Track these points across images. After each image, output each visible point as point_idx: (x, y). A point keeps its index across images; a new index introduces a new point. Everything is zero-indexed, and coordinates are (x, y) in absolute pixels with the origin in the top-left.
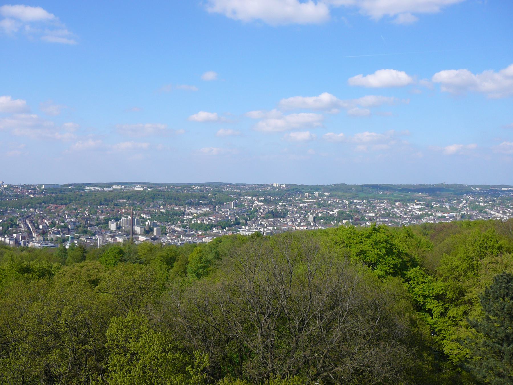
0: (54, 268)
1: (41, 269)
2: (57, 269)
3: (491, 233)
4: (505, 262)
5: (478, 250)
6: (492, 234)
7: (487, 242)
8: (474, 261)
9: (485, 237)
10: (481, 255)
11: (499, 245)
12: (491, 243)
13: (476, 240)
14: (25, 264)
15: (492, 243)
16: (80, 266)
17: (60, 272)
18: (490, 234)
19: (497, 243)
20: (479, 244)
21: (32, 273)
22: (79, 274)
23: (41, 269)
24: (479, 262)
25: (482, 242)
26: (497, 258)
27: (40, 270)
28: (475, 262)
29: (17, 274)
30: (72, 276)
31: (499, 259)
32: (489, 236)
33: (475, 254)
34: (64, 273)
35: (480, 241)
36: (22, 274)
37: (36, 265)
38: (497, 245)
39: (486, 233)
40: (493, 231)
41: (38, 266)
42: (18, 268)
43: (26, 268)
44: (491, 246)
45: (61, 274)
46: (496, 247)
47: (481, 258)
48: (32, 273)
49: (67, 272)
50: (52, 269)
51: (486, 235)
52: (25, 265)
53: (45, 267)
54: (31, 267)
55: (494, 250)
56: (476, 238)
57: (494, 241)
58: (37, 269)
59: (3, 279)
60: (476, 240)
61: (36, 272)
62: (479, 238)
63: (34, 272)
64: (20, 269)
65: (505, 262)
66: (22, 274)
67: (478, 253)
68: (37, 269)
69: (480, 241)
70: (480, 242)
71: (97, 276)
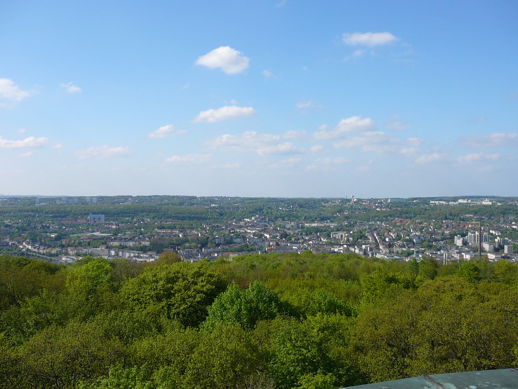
0: (418, 280)
1: (405, 280)
2: (420, 282)
14: (391, 275)
16: (443, 281)
17: (423, 285)
21: (398, 283)
22: (443, 288)
23: (405, 280)
27: (404, 281)
29: (384, 283)
30: (436, 290)
34: (428, 286)
36: (388, 283)
37: (401, 277)
41: (403, 277)
42: (385, 277)
43: (391, 278)
45: (424, 286)
48: (398, 283)
49: (430, 285)
50: (416, 281)
52: (391, 276)
53: (409, 279)
54: (396, 278)
58: (402, 280)
59: (371, 286)
61: (401, 283)
63: (399, 283)
64: (387, 279)
66: (389, 283)
68: (402, 280)
71: (462, 292)
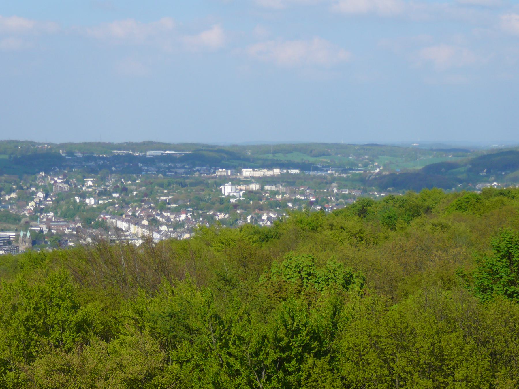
3: (58, 285)
4: (90, 365)
5: (23, 335)
6: (61, 287)
7: (48, 312)
8: (10, 370)
9: (42, 296)
10: (31, 353)
11: (79, 319)
12: (58, 314)
13: (15, 308)
15: (61, 314)
18: (55, 287)
19: (76, 312)
20: (23, 317)
24: (23, 375)
25: (33, 311)
26: (68, 357)
28: (11, 374)
31: (74, 359)
32: (52, 292)
33: (14, 349)
35: (26, 310)
38: (74, 319)
39: (44, 286)
40: (63, 277)
44: (58, 324)
46: (73, 323)
47: (30, 358)
51: (43, 292)
55: (67, 333)
56: (15, 301)
57: (66, 308)
60: (15, 308)
62: (25, 301)
65: (90, 365)
67: (22, 347)
69: (26, 310)
70: (27, 314)
